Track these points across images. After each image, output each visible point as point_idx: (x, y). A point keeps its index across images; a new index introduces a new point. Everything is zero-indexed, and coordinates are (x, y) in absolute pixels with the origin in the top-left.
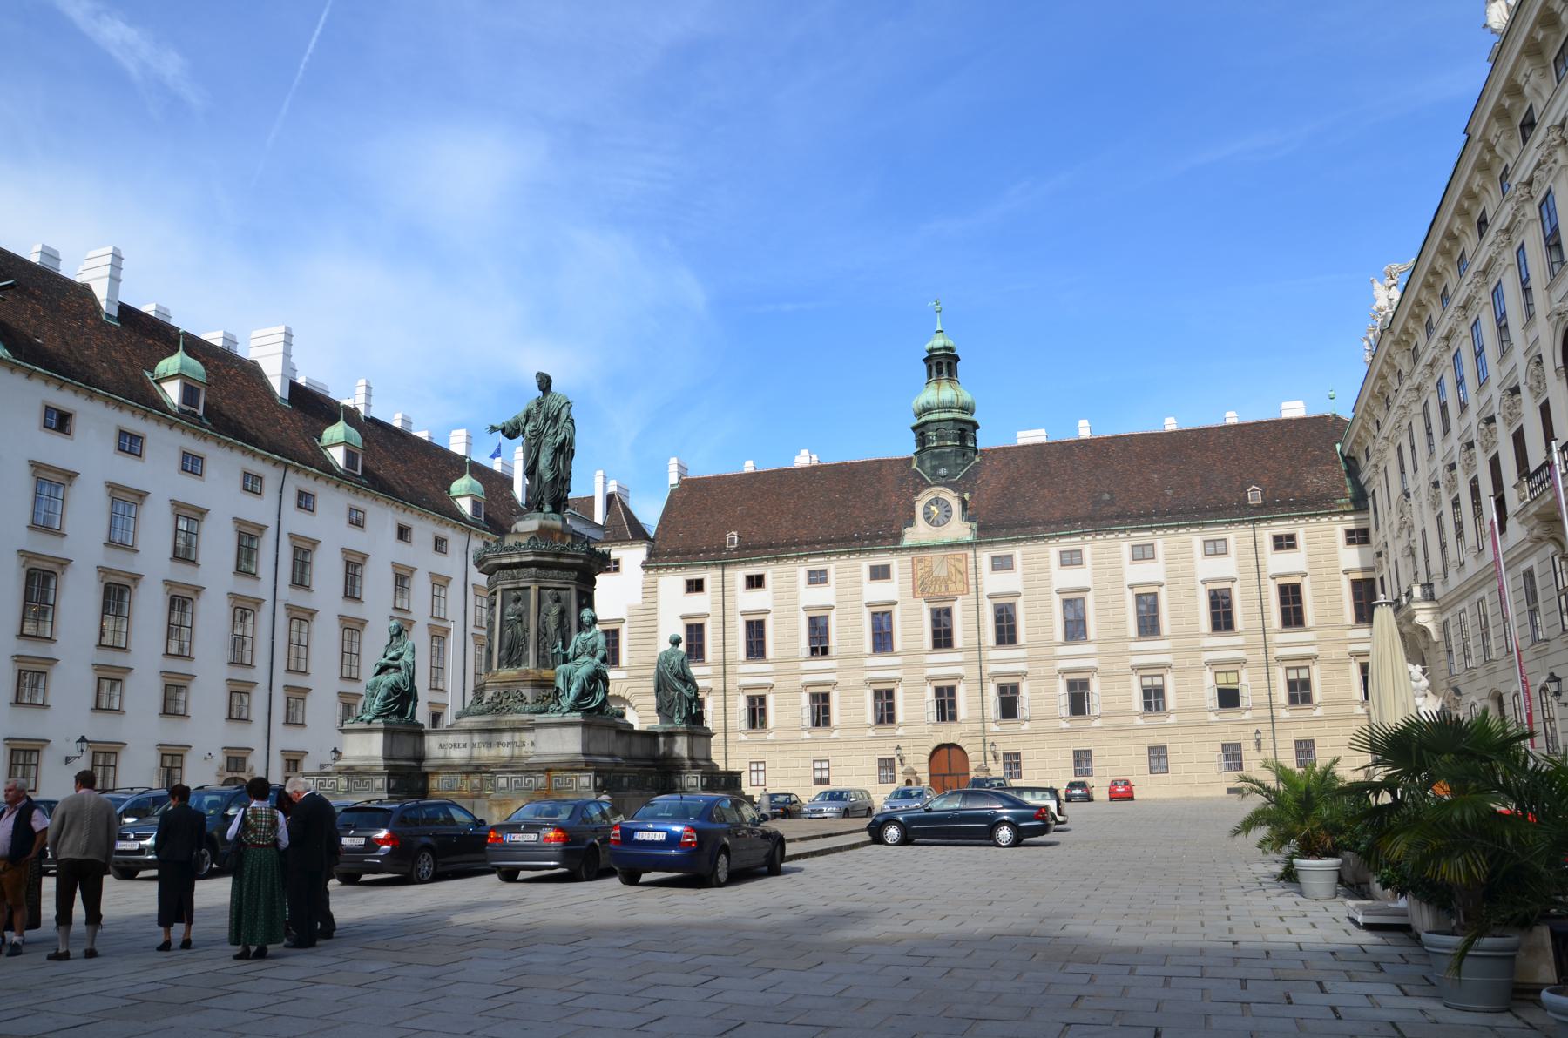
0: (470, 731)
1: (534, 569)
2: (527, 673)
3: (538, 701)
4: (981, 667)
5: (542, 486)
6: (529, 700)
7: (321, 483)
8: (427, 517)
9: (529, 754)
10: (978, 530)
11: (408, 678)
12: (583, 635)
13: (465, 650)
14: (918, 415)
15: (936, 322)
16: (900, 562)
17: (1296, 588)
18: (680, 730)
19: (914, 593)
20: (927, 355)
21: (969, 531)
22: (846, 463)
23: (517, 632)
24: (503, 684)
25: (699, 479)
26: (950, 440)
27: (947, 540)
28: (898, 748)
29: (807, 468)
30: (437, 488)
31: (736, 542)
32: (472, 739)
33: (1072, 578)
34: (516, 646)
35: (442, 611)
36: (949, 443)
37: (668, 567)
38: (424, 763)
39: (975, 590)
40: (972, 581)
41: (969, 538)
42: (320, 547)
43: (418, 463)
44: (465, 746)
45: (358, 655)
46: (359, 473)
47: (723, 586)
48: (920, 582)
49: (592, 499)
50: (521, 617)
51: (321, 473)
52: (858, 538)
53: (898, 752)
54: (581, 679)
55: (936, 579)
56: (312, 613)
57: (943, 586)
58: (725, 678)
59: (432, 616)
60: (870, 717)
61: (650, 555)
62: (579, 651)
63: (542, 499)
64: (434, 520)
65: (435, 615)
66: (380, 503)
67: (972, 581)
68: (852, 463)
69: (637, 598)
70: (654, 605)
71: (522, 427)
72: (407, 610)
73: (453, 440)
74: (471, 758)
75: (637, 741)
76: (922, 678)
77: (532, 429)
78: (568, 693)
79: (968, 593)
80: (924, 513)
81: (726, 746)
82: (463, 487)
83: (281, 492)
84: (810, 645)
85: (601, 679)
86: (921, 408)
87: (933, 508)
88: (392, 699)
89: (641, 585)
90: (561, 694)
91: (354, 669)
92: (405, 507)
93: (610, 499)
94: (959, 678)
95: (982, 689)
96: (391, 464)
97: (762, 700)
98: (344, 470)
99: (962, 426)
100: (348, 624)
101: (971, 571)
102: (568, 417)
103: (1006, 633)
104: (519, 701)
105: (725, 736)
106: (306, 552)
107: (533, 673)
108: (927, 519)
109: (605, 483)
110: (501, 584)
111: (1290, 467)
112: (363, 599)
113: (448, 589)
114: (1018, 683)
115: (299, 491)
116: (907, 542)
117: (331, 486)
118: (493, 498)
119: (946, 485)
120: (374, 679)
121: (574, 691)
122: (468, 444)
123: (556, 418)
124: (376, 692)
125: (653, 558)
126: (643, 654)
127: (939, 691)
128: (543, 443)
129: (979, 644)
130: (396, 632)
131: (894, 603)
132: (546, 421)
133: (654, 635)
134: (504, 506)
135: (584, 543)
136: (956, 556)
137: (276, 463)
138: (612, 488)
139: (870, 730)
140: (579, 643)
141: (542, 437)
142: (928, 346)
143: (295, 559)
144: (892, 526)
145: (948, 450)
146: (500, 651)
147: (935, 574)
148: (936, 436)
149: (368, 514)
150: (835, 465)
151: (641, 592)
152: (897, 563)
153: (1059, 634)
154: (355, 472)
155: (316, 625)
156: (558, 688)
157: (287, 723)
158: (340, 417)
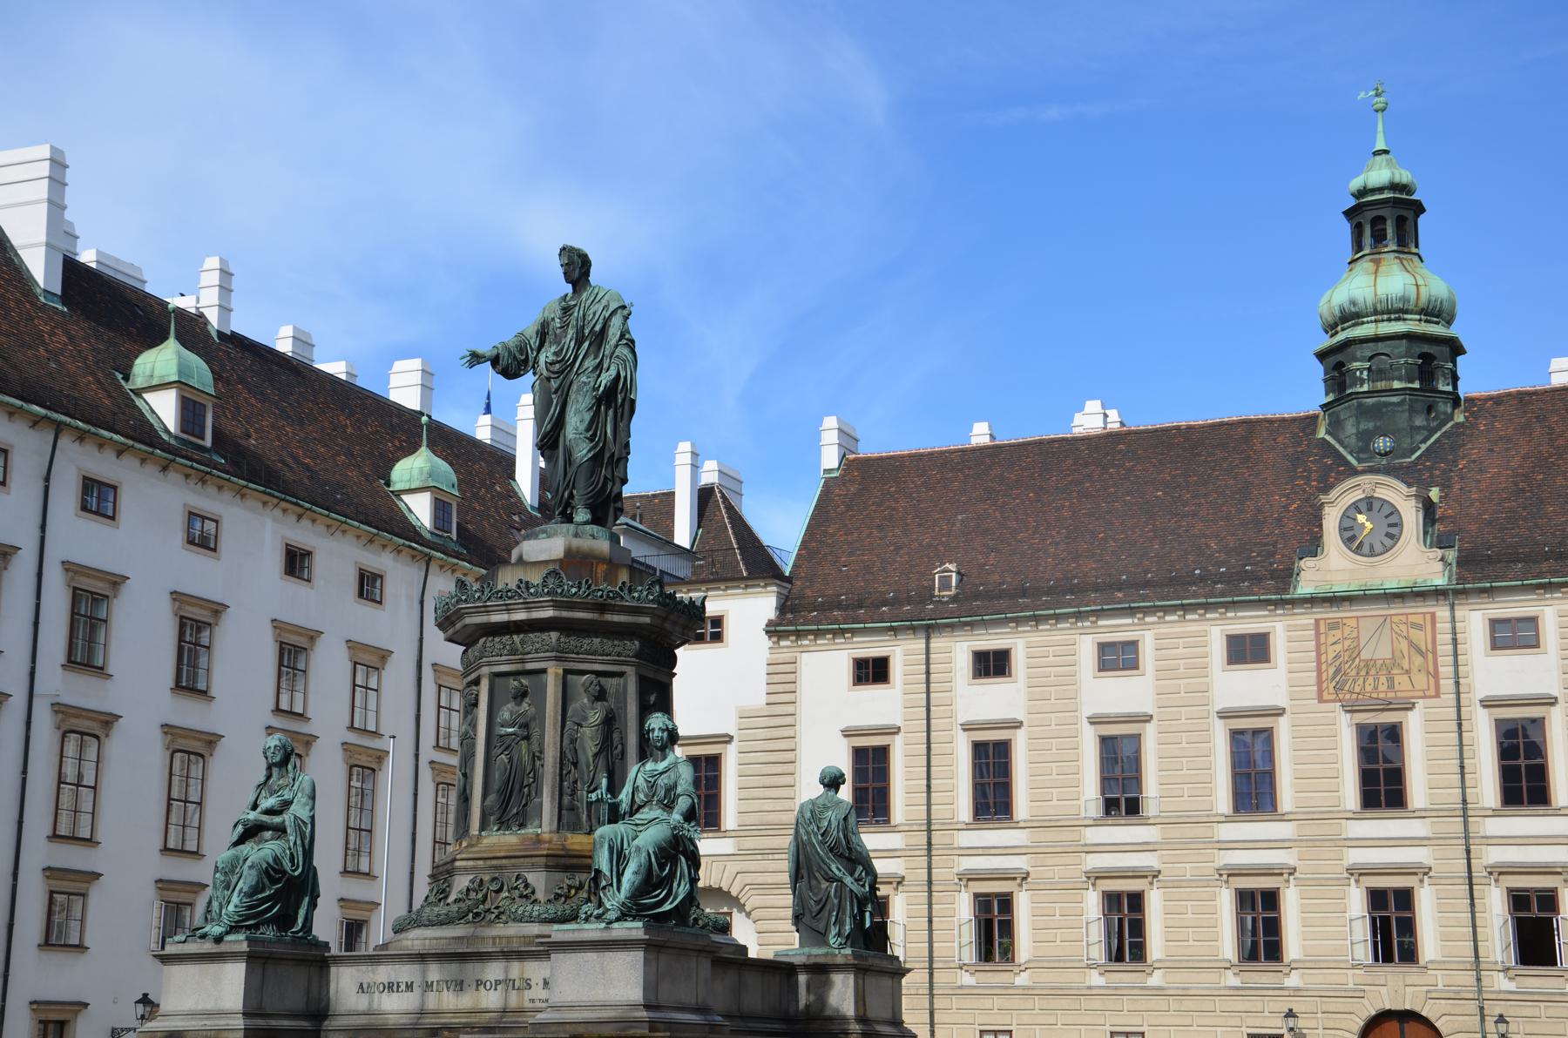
0: (422, 958)
1: (554, 635)
2: (538, 840)
3: (558, 897)
4: (1468, 852)
5: (571, 471)
6: (540, 895)
7: (130, 462)
8: (344, 532)
9: (538, 1005)
10: (1459, 564)
11: (300, 849)
12: (650, 766)
13: (416, 795)
14: (1331, 328)
15: (1375, 133)
18: (839, 960)
19: (1320, 691)
20: (1352, 202)
21: (1439, 566)
22: (1178, 428)
23: (520, 759)
24: (489, 863)
25: (881, 459)
26: (1400, 379)
27: (1391, 584)
28: (1290, 1014)
29: (1099, 437)
30: (366, 476)
31: (954, 584)
32: (424, 974)
34: (517, 787)
35: (371, 716)
36: (1397, 385)
37: (818, 634)
38: (326, 1023)
39: (1452, 688)
40: (1446, 670)
41: (1440, 581)
42: (128, 594)
43: (327, 424)
44: (409, 987)
45: (200, 804)
46: (208, 442)
47: (928, 673)
48: (1332, 670)
49: (669, 497)
50: (527, 728)
51: (130, 442)
52: (1202, 579)
53: (1291, 1023)
54: (644, 854)
55: (1367, 666)
56: (108, 721)
57: (1383, 679)
58: (930, 856)
59: (352, 727)
60: (1228, 945)
61: (782, 608)
62: (641, 797)
63: (571, 496)
64: (358, 537)
65: (356, 725)
66: (250, 502)
67: (1446, 670)
68: (1189, 428)
69: (756, 696)
70: (789, 709)
71: (532, 356)
72: (301, 715)
73: (395, 381)
74: (422, 1013)
75: (753, 980)
76: (1339, 870)
77: (551, 358)
78: (619, 881)
79: (1437, 695)
80: (1342, 529)
81: (932, 995)
82: (415, 472)
83: (47, 479)
84: (1103, 793)
85: (685, 853)
86: (1337, 313)
87: (1361, 518)
88: (267, 893)
89: (764, 669)
90: (604, 883)
91: (192, 834)
92: (300, 510)
93: (705, 497)
95: (1472, 898)
96: (273, 426)
97: (1006, 902)
98: (176, 438)
99: (1426, 348)
100: (182, 743)
102: (622, 336)
104: (521, 896)
105: (931, 975)
106: (98, 599)
107: (550, 842)
109: (695, 467)
110: (490, 664)
112: (213, 692)
113: (384, 673)
114: (1554, 890)
115: (85, 478)
116: (1305, 587)
117: (151, 469)
118: (475, 495)
119: (1389, 471)
120: (233, 851)
121: (628, 877)
122: (426, 388)
123: (600, 337)
124: (235, 878)
125: (789, 616)
126: (768, 805)
127: (1377, 898)
128: (574, 387)
129: (1464, 801)
130: (277, 759)
131: (1279, 712)
132: (579, 343)
134: (496, 508)
135: (652, 584)
136: (1412, 619)
137: (36, 422)
138: (709, 476)
139: (1229, 973)
140: (640, 782)
141: (572, 375)
142: (1356, 183)
143: (74, 613)
144: (1273, 554)
145: (1395, 399)
146: (485, 795)
147: (1365, 655)
148: (1369, 369)
149: (225, 526)
150: (1156, 430)
151: (764, 688)
152: (1282, 629)
154: (200, 442)
155: (116, 745)
156: (598, 872)
157: (47, 944)
158: (169, 333)
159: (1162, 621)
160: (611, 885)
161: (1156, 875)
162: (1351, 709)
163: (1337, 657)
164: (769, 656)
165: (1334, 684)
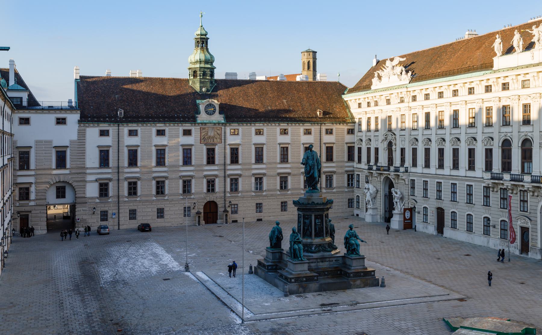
0: (317, 259)
16: (195, 129)
17: (332, 147)
21: (223, 119)
27: (214, 122)
28: (195, 203)
33: (260, 139)
39: (224, 142)
40: (223, 138)
41: (223, 121)
44: (315, 262)
47: (118, 134)
48: (203, 137)
53: (195, 205)
57: (212, 140)
60: (181, 191)
61: (81, 117)
67: (223, 138)
70: (84, 141)
79: (221, 143)
80: (205, 109)
94: (216, 176)
101: (223, 134)
103: (235, 159)
108: (206, 112)
111: (329, 102)
126: (78, 163)
133: (83, 154)
144: (189, 113)
153: (253, 160)
156: (355, 249)
159: (170, 126)
160: (357, 250)
161: (167, 177)
162: (206, 145)
163: (204, 135)
164: (78, 128)
165: (203, 140)
